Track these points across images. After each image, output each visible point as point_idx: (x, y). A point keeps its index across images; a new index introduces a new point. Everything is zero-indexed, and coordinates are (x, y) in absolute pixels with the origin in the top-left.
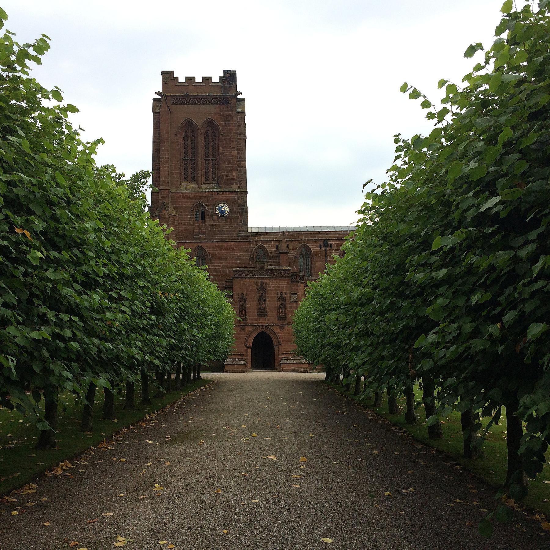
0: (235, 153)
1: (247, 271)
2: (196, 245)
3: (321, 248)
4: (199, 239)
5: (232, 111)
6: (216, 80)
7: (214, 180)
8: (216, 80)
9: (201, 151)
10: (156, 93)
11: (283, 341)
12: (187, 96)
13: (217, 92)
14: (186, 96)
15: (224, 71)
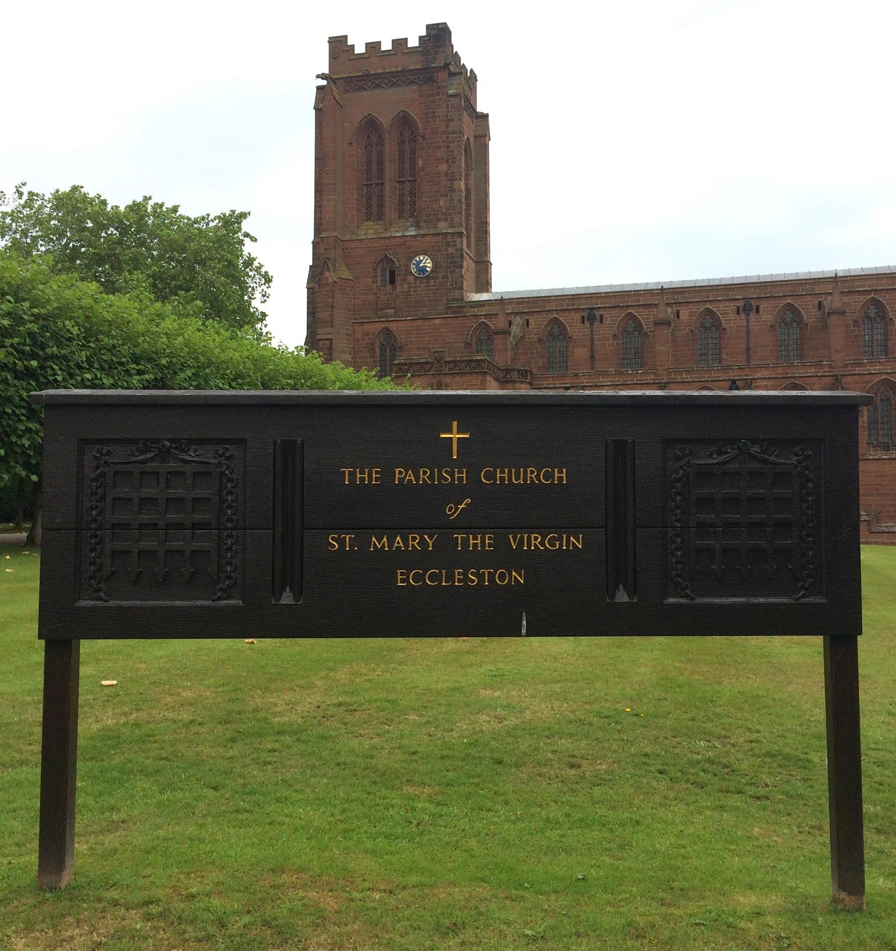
0: (443, 168)
1: (417, 364)
2: (379, 327)
3: (583, 323)
4: (385, 316)
5: (438, 94)
6: (413, 43)
7: (412, 216)
8: (413, 43)
9: (390, 170)
10: (318, 76)
12: (367, 76)
13: (415, 64)
14: (366, 77)
15: (427, 26)
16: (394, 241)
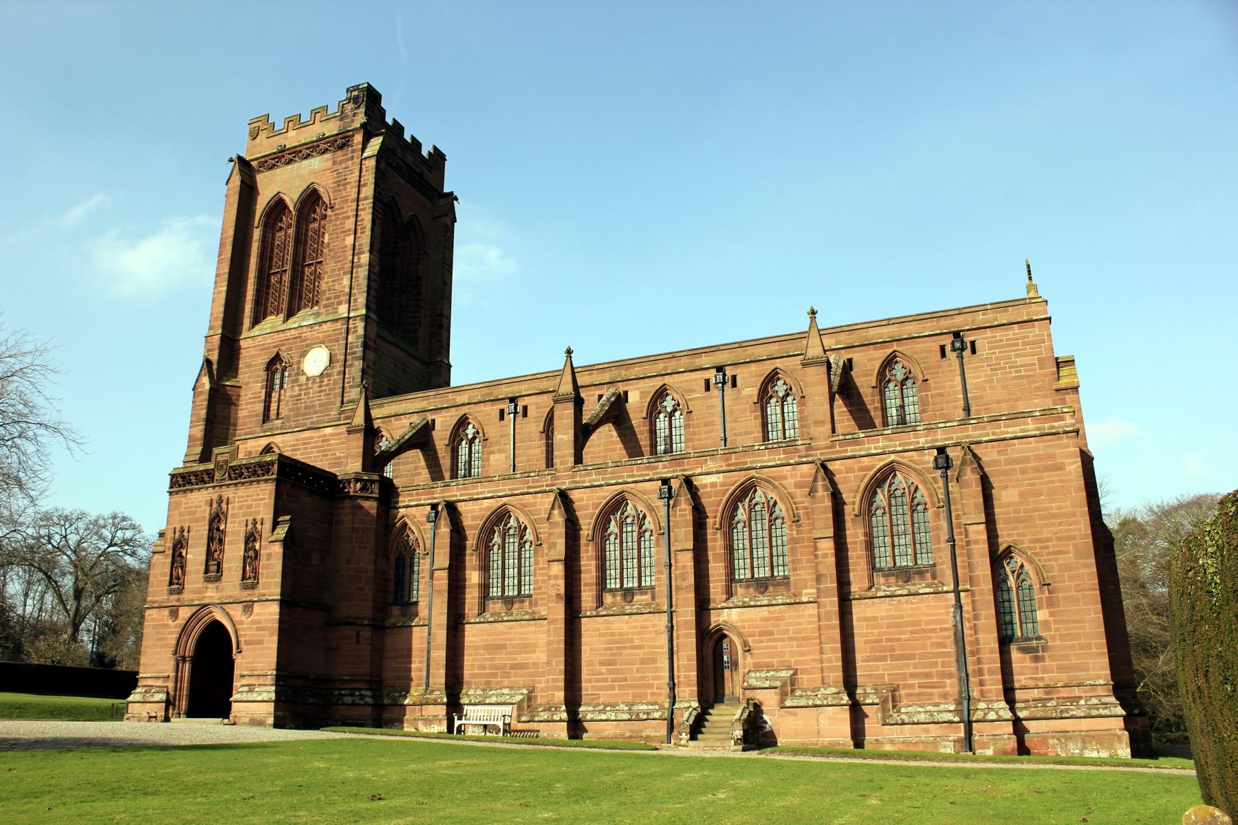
2: (263, 442)
11: (247, 643)
16: (288, 334)
